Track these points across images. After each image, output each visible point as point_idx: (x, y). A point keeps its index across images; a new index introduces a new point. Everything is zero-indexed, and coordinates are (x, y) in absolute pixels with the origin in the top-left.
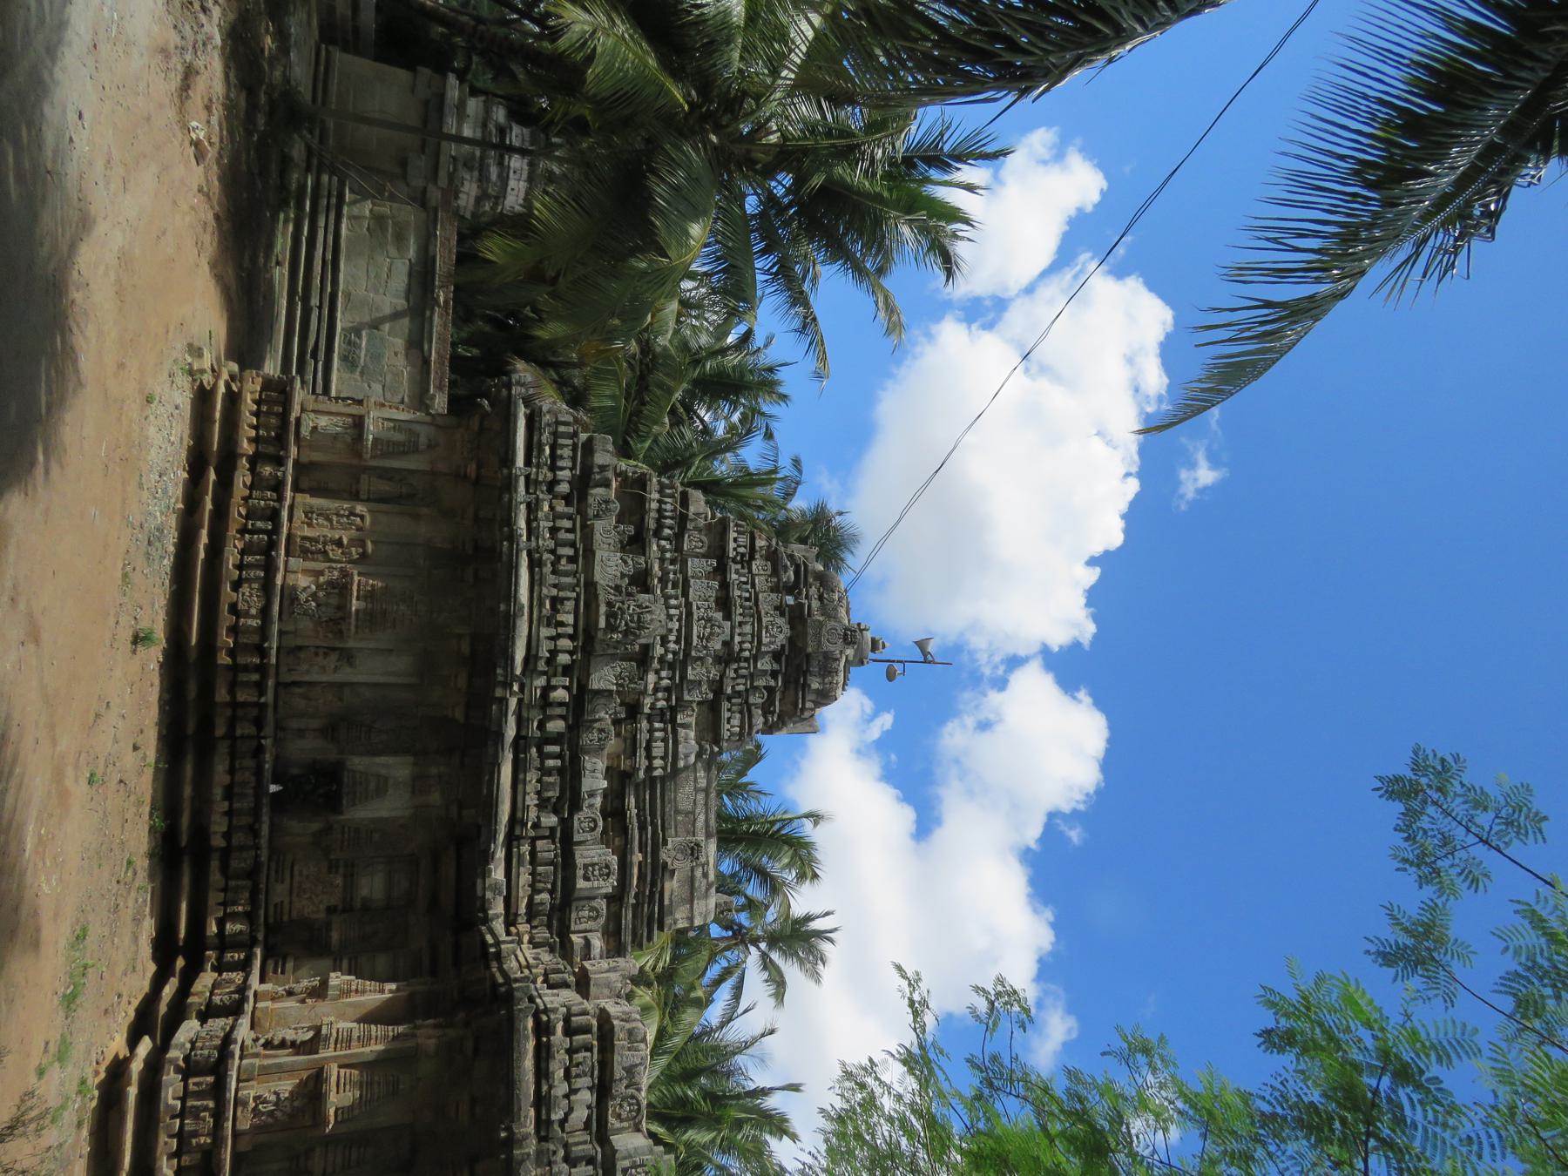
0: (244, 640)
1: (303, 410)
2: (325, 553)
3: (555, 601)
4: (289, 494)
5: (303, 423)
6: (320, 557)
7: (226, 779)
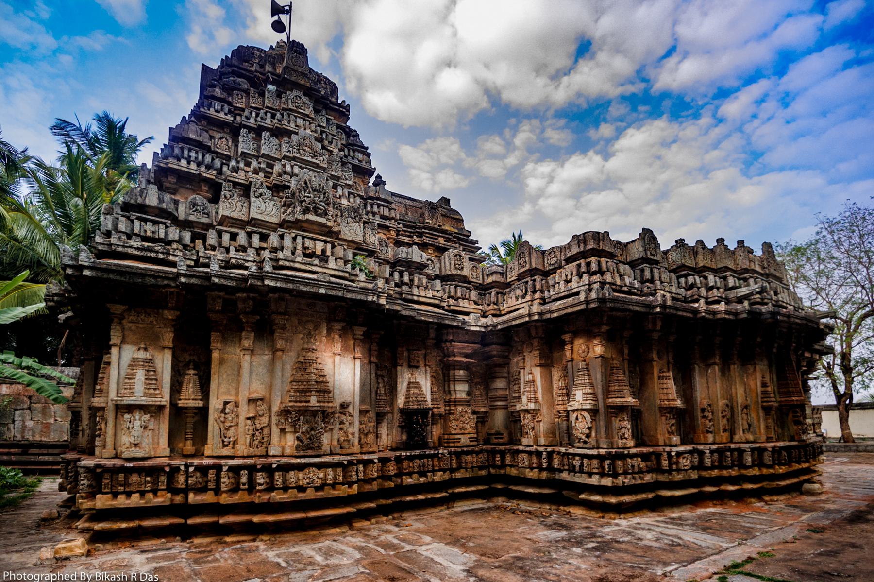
0: (340, 479)
1: (116, 457)
2: (262, 429)
3: (312, 255)
4: (206, 462)
5: (132, 455)
6: (266, 431)
7: (415, 476)
